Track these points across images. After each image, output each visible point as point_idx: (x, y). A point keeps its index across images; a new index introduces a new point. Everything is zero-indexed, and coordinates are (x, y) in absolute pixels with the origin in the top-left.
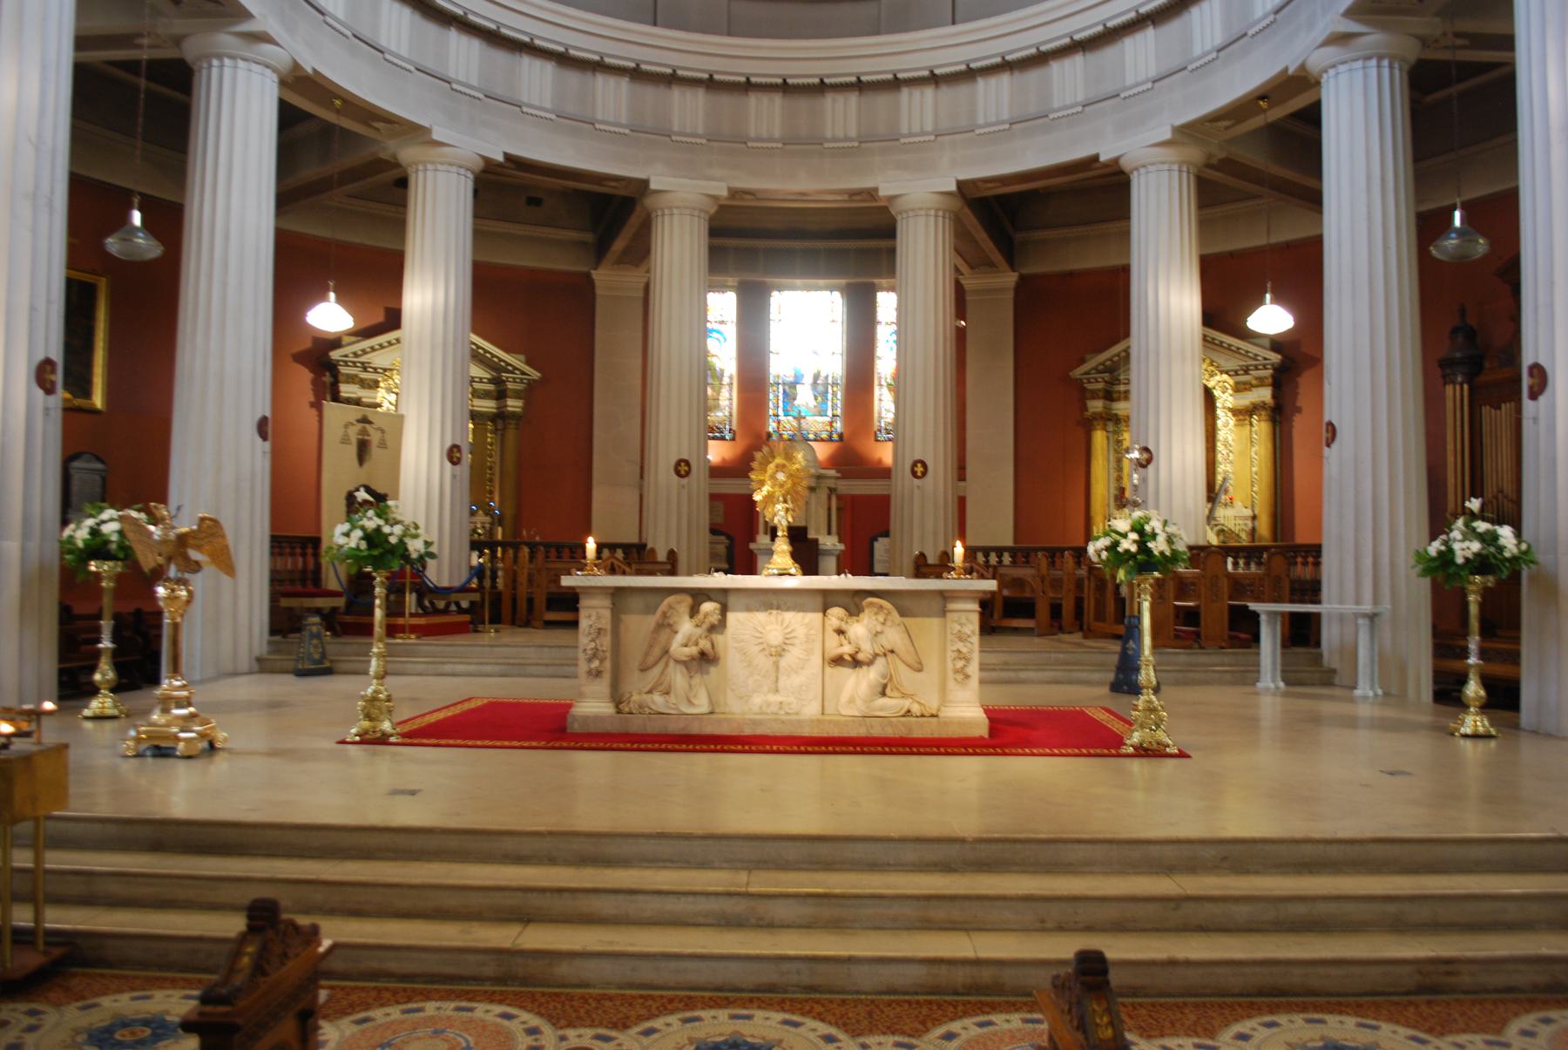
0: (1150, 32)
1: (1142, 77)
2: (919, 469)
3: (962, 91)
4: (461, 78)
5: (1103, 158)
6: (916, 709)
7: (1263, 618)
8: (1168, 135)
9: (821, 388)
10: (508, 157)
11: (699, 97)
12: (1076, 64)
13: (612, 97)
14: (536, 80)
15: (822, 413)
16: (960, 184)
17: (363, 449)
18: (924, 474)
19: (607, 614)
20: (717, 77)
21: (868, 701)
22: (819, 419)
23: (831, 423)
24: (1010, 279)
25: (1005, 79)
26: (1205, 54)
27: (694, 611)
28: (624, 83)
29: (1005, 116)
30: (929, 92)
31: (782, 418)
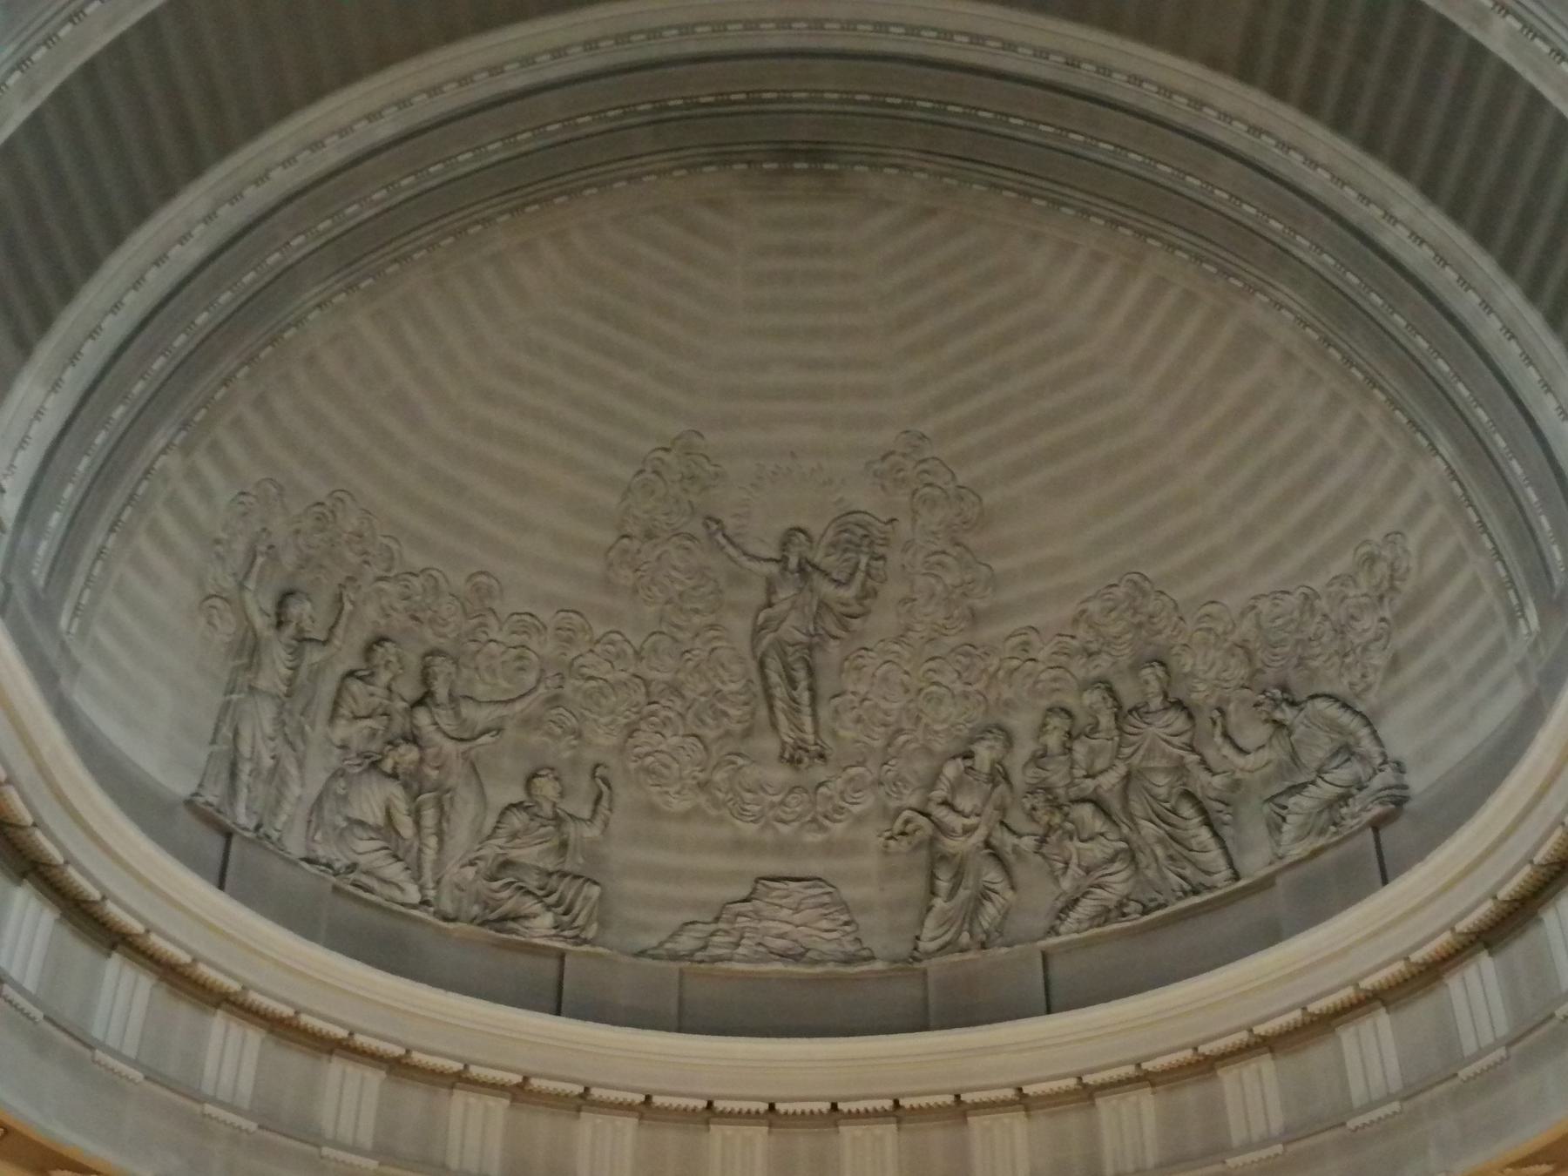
20: (658, 1100)
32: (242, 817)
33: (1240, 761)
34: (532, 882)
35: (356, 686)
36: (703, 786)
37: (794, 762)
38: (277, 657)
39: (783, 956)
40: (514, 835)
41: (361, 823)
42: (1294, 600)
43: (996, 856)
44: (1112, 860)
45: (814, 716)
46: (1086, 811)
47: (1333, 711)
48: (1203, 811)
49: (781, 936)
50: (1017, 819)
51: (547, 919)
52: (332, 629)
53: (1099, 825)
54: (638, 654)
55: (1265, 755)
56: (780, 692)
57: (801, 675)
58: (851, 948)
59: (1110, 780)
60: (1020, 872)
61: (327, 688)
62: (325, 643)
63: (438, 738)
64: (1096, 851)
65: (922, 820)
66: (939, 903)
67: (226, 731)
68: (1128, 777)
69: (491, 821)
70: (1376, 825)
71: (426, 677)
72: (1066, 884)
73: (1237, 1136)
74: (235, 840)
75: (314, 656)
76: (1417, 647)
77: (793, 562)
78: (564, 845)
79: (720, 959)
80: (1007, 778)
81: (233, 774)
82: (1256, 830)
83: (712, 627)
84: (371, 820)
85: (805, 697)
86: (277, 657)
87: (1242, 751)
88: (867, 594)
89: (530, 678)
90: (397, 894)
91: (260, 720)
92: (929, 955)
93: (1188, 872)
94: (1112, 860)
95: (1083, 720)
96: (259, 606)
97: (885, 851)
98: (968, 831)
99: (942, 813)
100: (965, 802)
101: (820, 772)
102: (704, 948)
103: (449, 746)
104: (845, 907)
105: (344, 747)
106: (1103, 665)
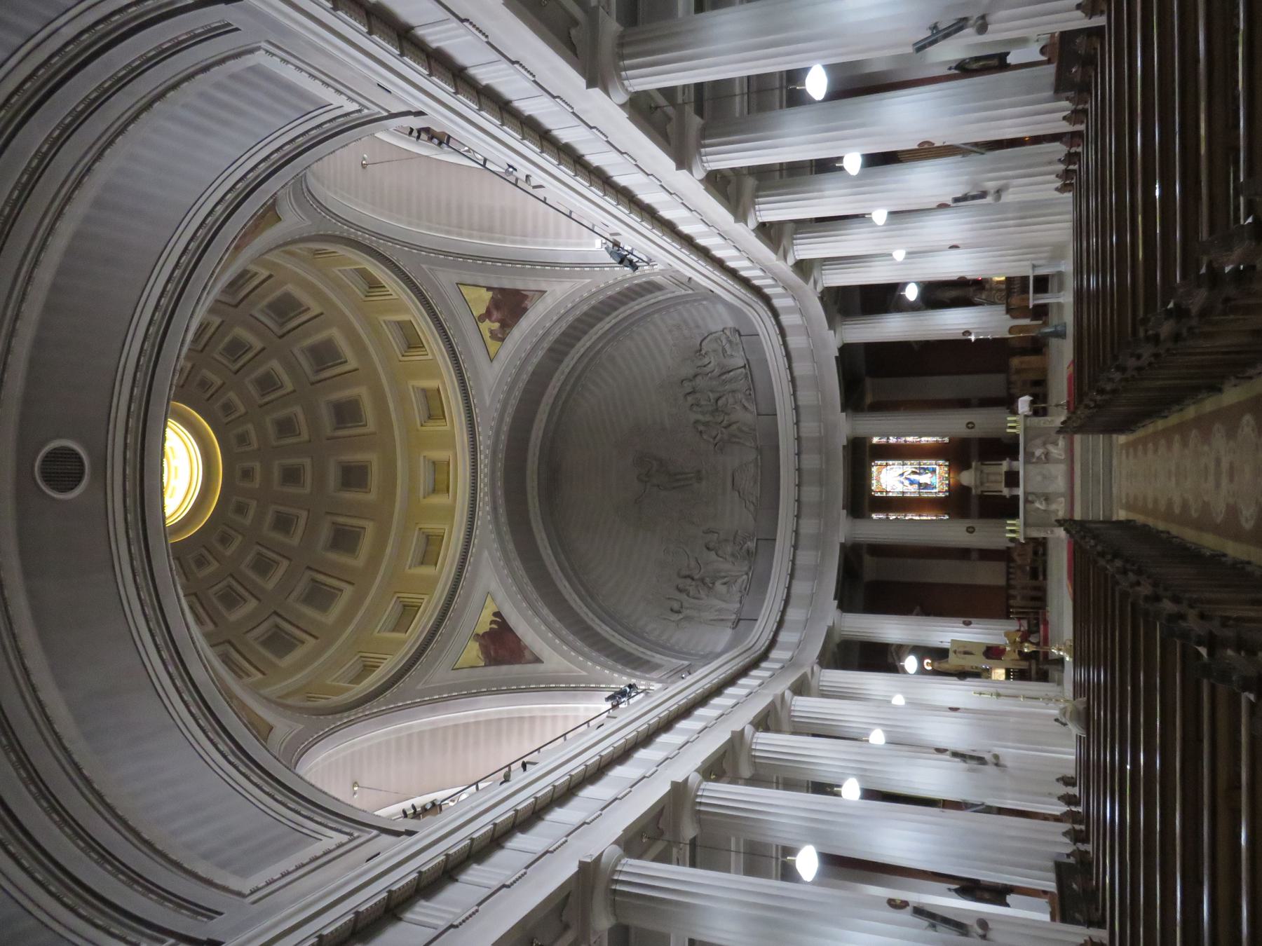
3: (802, 411)
5: (837, 355)
8: (832, 332)
10: (835, 599)
11: (803, 522)
13: (806, 558)
14: (800, 588)
15: (934, 471)
22: (937, 472)
24: (868, 382)
28: (798, 552)
30: (802, 424)
31: (937, 490)
32: (734, 617)
33: (712, 364)
34: (737, 548)
35: (691, 594)
38: (688, 612)
39: (755, 483)
43: (729, 425)
46: (720, 403)
48: (725, 373)
50: (719, 420)
51: (749, 543)
53: (724, 399)
59: (711, 395)
66: (741, 441)
68: (712, 391)
69: (721, 559)
70: (740, 335)
71: (685, 577)
74: (741, 617)
75: (686, 604)
79: (757, 498)
80: (708, 422)
81: (722, 620)
86: (688, 612)
87: (710, 363)
90: (746, 581)
96: (676, 617)
98: (722, 433)
100: (714, 434)
103: (702, 571)
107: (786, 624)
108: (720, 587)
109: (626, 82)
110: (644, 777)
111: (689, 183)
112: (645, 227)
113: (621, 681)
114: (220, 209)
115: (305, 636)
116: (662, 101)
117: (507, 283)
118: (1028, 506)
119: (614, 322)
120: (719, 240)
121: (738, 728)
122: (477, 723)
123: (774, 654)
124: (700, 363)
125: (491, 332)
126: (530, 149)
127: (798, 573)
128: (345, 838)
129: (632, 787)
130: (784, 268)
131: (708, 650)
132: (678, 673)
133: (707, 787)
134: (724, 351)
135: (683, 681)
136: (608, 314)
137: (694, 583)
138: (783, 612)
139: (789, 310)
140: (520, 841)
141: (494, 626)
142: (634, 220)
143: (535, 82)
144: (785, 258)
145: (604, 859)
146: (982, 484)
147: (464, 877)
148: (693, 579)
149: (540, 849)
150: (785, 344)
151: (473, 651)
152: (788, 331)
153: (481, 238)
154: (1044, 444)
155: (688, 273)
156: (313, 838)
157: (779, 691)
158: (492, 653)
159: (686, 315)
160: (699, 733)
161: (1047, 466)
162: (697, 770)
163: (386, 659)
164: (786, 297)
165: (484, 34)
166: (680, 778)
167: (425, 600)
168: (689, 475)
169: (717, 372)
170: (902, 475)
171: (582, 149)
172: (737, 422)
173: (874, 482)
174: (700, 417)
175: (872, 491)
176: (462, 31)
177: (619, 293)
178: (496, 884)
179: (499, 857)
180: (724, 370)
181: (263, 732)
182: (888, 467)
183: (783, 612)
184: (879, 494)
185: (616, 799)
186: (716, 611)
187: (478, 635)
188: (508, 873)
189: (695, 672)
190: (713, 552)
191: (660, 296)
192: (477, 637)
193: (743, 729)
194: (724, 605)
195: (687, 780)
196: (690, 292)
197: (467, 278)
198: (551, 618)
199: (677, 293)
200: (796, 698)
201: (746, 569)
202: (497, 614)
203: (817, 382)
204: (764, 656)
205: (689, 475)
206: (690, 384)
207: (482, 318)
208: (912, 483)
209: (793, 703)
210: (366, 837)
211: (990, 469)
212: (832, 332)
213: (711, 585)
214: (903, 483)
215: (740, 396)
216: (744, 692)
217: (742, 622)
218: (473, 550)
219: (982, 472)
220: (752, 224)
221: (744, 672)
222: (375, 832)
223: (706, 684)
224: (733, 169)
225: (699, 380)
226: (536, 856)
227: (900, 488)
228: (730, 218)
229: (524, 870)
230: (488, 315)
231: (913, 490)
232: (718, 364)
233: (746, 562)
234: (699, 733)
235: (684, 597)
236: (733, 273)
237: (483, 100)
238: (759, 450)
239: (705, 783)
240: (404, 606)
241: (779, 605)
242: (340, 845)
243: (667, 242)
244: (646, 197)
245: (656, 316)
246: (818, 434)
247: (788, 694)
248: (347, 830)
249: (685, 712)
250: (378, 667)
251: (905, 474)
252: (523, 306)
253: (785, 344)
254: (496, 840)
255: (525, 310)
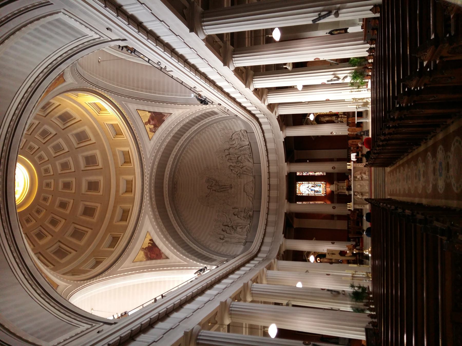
0: (265, 134)
1: (272, 135)
2: (334, 168)
3: (270, 162)
4: (271, 240)
5: (284, 141)
6: (367, 170)
7: (358, 121)
8: (282, 132)
9: (316, 186)
10: (283, 234)
11: (271, 204)
12: (268, 145)
13: (272, 218)
14: (270, 229)
15: (320, 186)
16: (285, 162)
17: (333, 254)
18: (334, 167)
19: (356, 205)
21: (366, 175)
23: (322, 184)
24: (295, 151)
25: (269, 155)
26: (271, 127)
27: (356, 195)
28: (269, 216)
29: (275, 155)
30: (270, 167)
31: (321, 193)
32: (244, 241)
34: (245, 214)
35: (228, 232)
36: (234, 197)
37: (232, 188)
39: (253, 189)
40: (241, 216)
41: (242, 231)
42: (222, 138)
44: (244, 156)
45: (227, 186)
46: (239, 158)
47: (234, 135)
48: (241, 147)
49: (250, 189)
51: (250, 212)
52: (223, 235)
53: (241, 157)
54: (221, 204)
55: (236, 141)
56: (225, 189)
57: (223, 187)
58: (251, 182)
59: (236, 156)
60: (245, 165)
61: (228, 235)
62: (224, 235)
63: (232, 224)
64: (243, 158)
65: (238, 175)
67: (236, 243)
68: (236, 154)
70: (247, 133)
72: (246, 161)
73: (274, 147)
74: (247, 241)
75: (226, 236)
76: (230, 127)
77: (211, 188)
78: (241, 211)
80: (235, 166)
81: (240, 242)
82: (244, 143)
83: (217, 196)
84: (241, 230)
85: (225, 187)
88: (214, 180)
89: (224, 215)
90: (249, 228)
91: (233, 240)
92: (253, 174)
93: (247, 149)
94: (244, 156)
95: (229, 158)
96: (222, 241)
97: (241, 179)
98: (240, 170)
99: (238, 173)
100: (237, 170)
101: (233, 185)
102: (252, 197)
103: (232, 223)
104: (247, 183)
105: (234, 233)
106: (224, 156)
107: (264, 244)
108: (239, 230)
109: (205, 31)
110: (209, 300)
111: (228, 71)
112: (211, 89)
113: (202, 266)
114: (41, 75)
115: (72, 251)
116: (217, 39)
117: (157, 110)
118: (355, 196)
119: (198, 126)
120: (239, 95)
121: (246, 282)
122: (142, 284)
123: (260, 255)
124: (231, 143)
125: (150, 129)
126: (167, 56)
127: (269, 224)
128: (89, 326)
129: (205, 304)
130: (264, 106)
131: (234, 254)
132: (222, 263)
133: (234, 304)
134: (241, 138)
135: (224, 265)
136: (196, 123)
137: (229, 228)
138: (263, 239)
139: (266, 123)
140: (160, 325)
141: (150, 245)
142: (207, 85)
143: (170, 29)
144: (264, 103)
145: (194, 330)
146: (338, 190)
147: (138, 339)
148: (228, 226)
149: (168, 328)
150: (264, 136)
151: (142, 254)
152: (265, 131)
153: (146, 92)
154: (361, 173)
155: (228, 107)
156: (76, 326)
157: (262, 268)
158: (149, 256)
159: (226, 124)
160: (231, 284)
161: (362, 182)
162: (230, 297)
163: (105, 259)
164: (264, 118)
165: (150, 9)
166: (223, 300)
167: (122, 235)
168: (227, 186)
169: (238, 147)
170: (308, 187)
171: (187, 57)
172: (246, 166)
173: (297, 190)
174: (232, 164)
175: (297, 193)
176: (142, 8)
177: (201, 115)
178: (151, 341)
179: (152, 331)
180: (240, 146)
181: (55, 286)
182: (303, 184)
183: (263, 239)
184: (299, 195)
185: (199, 309)
186: (237, 239)
187: (143, 248)
188: (156, 337)
189: (229, 261)
190: (236, 216)
191: (216, 117)
192: (142, 249)
193: (248, 282)
194: (240, 236)
195: (226, 301)
196: (228, 115)
197: (141, 107)
198: (173, 241)
199: (223, 116)
200: (268, 271)
201: (249, 222)
202: (151, 240)
203: (276, 151)
204: (256, 256)
205: (227, 186)
206: (227, 151)
207: (146, 124)
208: (312, 190)
209: (267, 273)
210: (98, 326)
211: (341, 184)
212: (282, 132)
213: (235, 229)
214: (308, 190)
215: (247, 156)
216: (248, 269)
217: (248, 243)
218: (142, 215)
219: (338, 185)
220: (252, 89)
221: (248, 262)
222: (102, 324)
223: (233, 266)
224: (245, 67)
225: (231, 150)
226: (167, 331)
227: (307, 192)
228: (243, 86)
229: (162, 336)
230: (149, 122)
231: (312, 193)
232: (239, 144)
233: (249, 220)
234: (231, 284)
235: (225, 233)
236: (244, 108)
237: (149, 35)
238: (254, 177)
239: (233, 302)
240: (113, 238)
241: (261, 236)
242: (87, 329)
243: (219, 95)
244: (212, 77)
245: (215, 125)
246: (276, 171)
247: (265, 269)
248: (90, 323)
249: (226, 276)
250: (102, 262)
251: (309, 187)
252: (163, 119)
253: (264, 136)
254: (151, 324)
255: (164, 121)
